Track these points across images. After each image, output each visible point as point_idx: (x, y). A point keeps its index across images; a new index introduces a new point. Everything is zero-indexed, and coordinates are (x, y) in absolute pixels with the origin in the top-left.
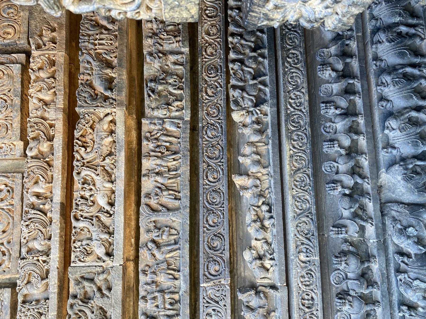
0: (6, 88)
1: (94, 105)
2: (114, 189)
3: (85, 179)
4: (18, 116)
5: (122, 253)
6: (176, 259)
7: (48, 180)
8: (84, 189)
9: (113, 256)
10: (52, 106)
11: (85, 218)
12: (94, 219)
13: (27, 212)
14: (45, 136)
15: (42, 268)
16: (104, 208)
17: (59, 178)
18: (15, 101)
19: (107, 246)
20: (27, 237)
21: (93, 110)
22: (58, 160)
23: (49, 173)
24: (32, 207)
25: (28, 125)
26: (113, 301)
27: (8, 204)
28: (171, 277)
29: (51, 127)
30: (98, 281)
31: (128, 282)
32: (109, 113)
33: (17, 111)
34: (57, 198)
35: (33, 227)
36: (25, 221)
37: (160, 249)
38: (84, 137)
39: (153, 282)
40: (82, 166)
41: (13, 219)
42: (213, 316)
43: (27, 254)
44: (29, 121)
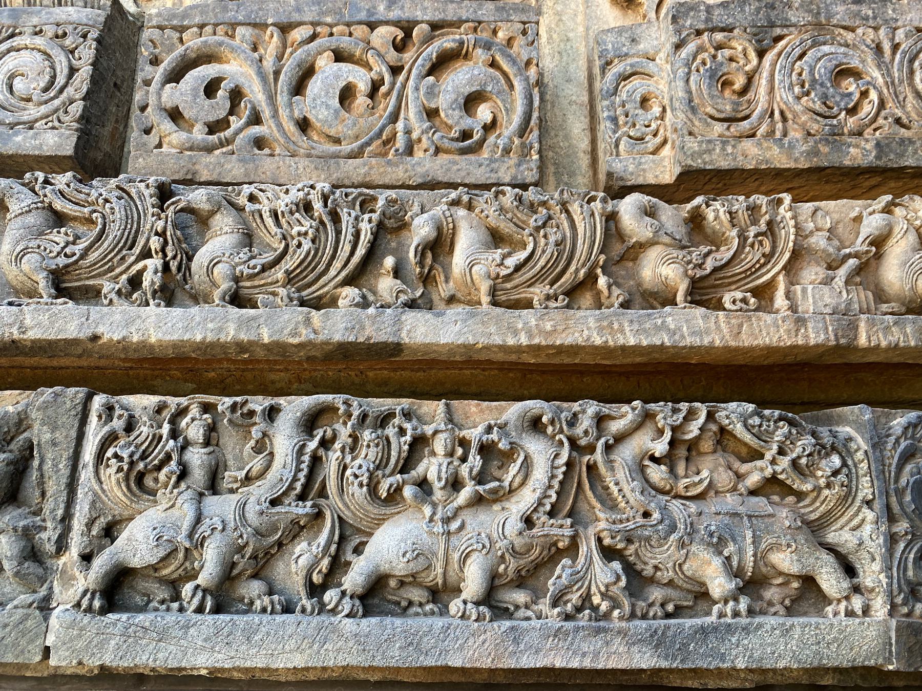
0: (909, 107)
1: (894, 499)
2: (455, 606)
3: (508, 456)
4: (789, 156)
7: (508, 285)
8: (460, 451)
9: (103, 611)
10: (863, 296)
11: (316, 460)
12: (304, 509)
13: (366, 204)
14: (715, 270)
15: (111, 269)
16: (358, 551)
17: (516, 333)
18: (857, 146)
19: (165, 572)
20: (257, 206)
21: (865, 489)
22: (600, 329)
23: (538, 292)
24: (390, 223)
25: (761, 200)
27: (415, 136)
29: (757, 292)
32: (850, 571)
33: (815, 152)
34: (421, 330)
35: (296, 229)
36: (325, 198)
38: (719, 442)
40: (573, 442)
41: (352, 156)
43: (182, 210)
44: (780, 202)
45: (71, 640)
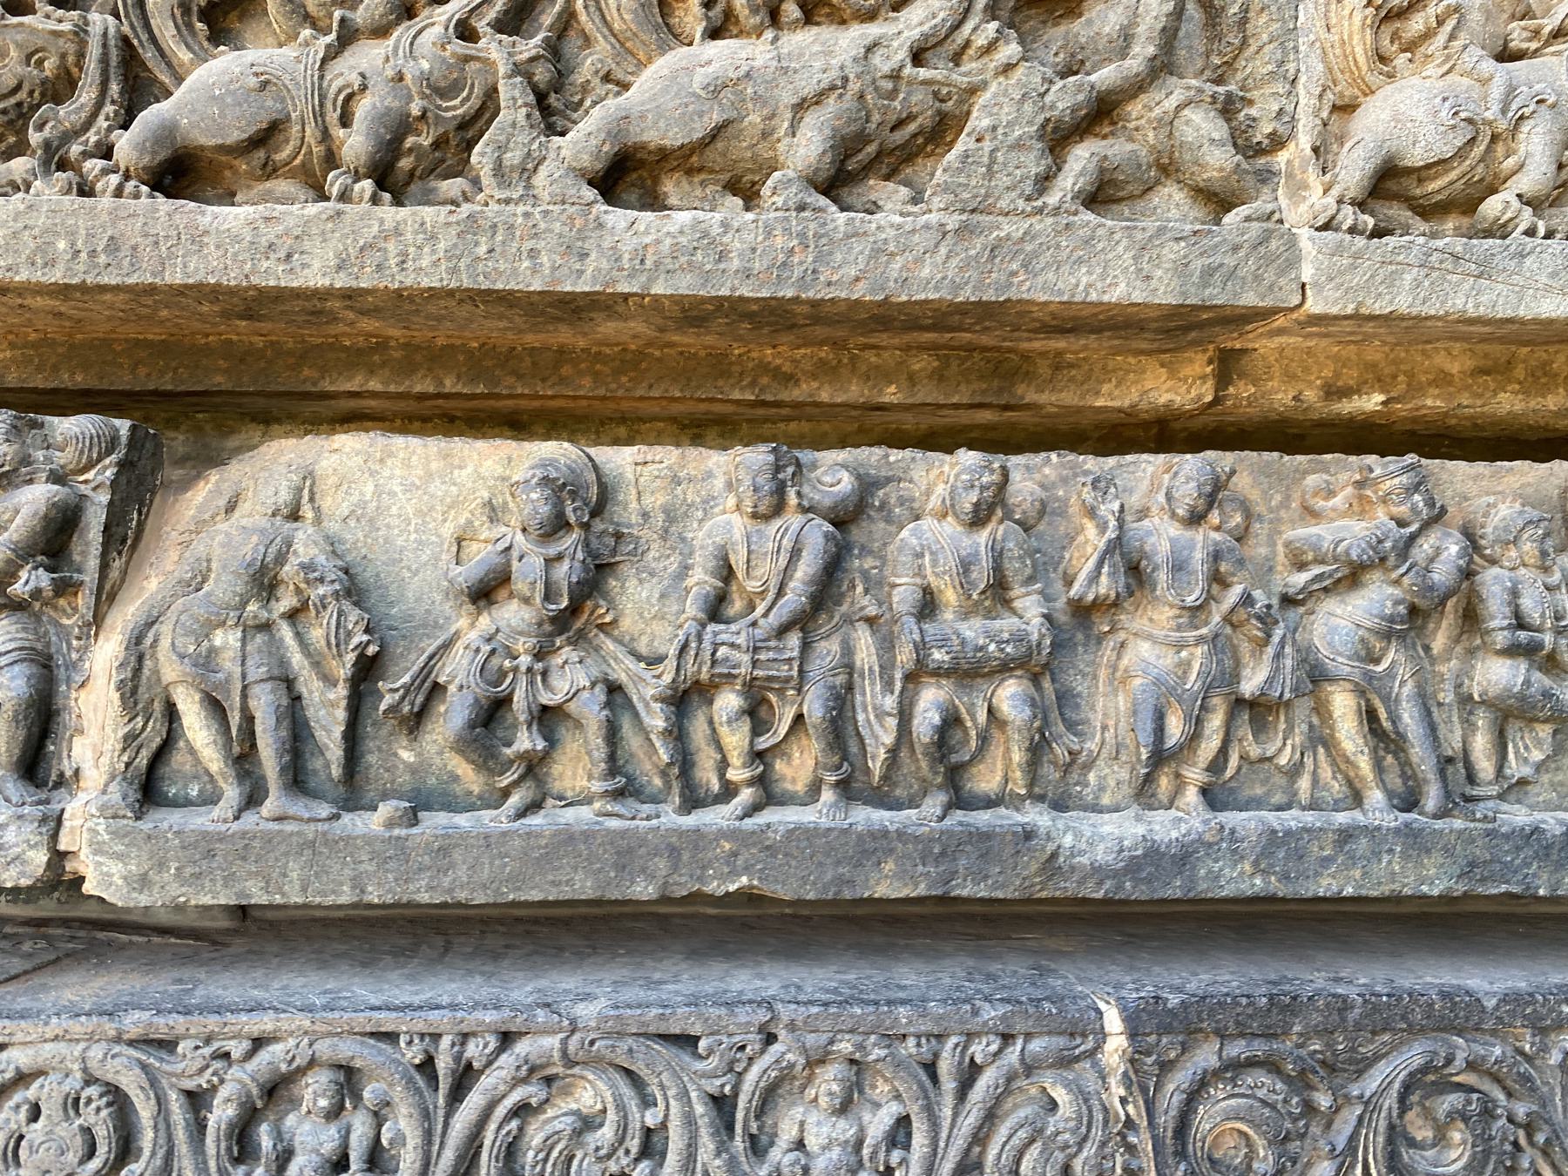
5: (1403, 303)
6: (1294, 771)
26: (1010, 228)
28: (1175, 728)
30: (1171, 103)
31: (1057, 368)
37: (1402, 636)
39: (1136, 572)
42: (845, 1129)
45: (1341, 273)
